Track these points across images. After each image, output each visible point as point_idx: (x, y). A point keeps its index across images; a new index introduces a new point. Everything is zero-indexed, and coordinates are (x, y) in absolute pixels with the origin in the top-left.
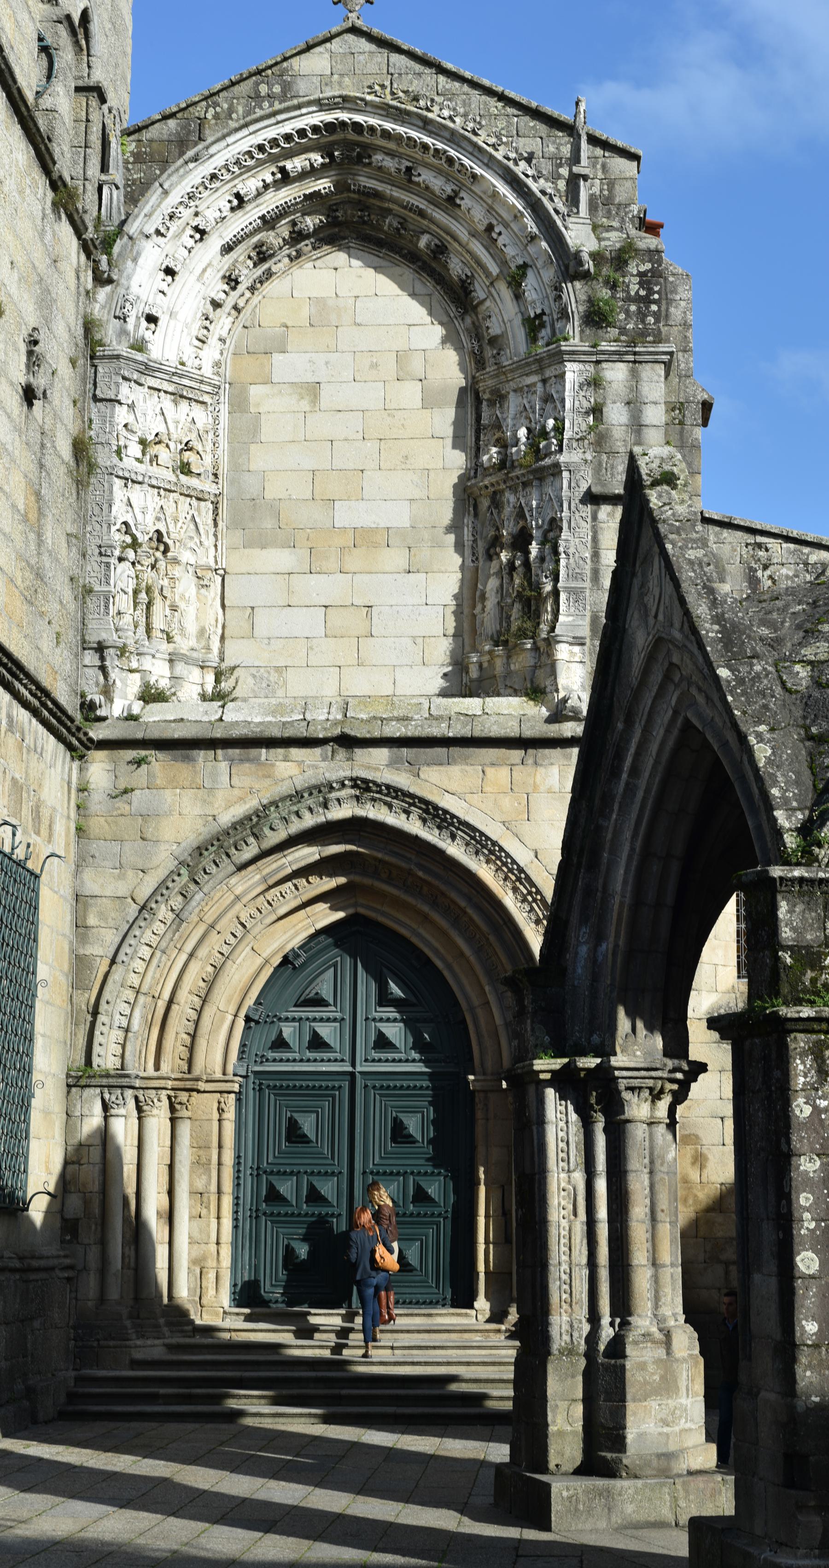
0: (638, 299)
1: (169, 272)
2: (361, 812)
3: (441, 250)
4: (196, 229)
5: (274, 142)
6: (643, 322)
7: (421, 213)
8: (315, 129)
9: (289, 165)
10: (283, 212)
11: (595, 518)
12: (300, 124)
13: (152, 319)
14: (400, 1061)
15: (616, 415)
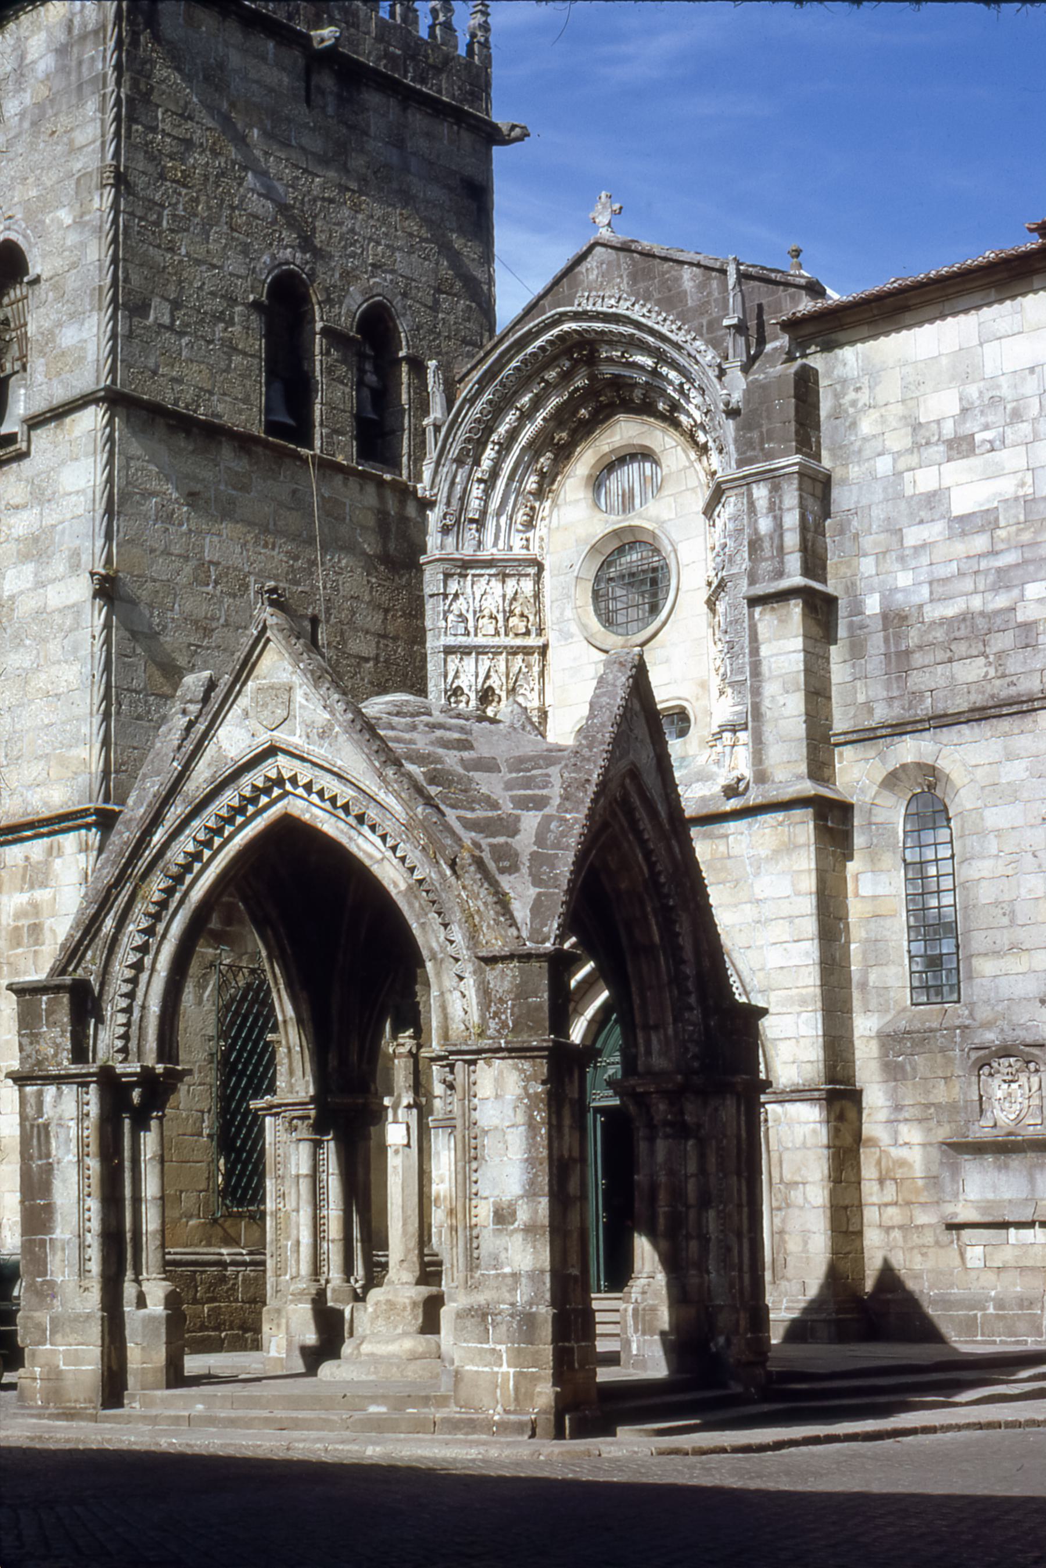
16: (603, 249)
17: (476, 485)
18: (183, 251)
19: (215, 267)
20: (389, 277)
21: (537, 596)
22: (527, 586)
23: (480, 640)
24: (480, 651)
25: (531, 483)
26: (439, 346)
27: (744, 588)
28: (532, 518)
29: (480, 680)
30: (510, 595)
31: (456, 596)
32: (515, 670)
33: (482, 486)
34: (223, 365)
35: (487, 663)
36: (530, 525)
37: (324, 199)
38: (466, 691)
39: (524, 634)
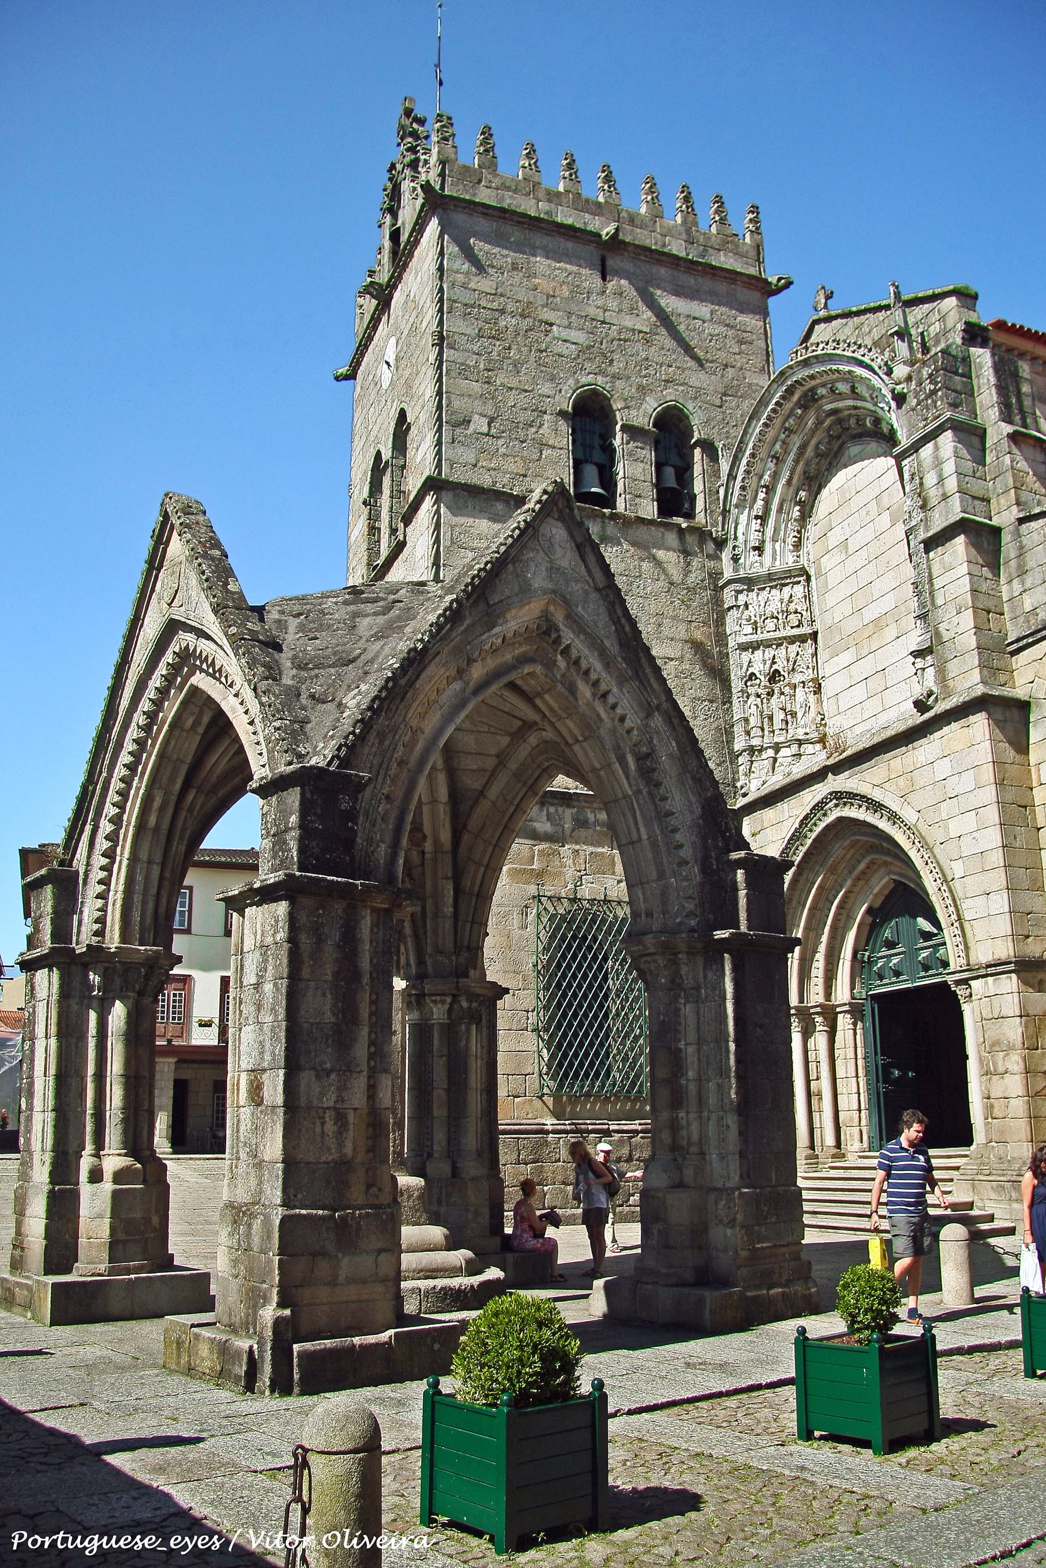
0: (933, 392)
1: (757, 517)
2: (839, 814)
3: (877, 421)
4: (763, 487)
5: (769, 418)
6: (935, 407)
7: (855, 408)
8: (783, 397)
9: (787, 425)
10: (803, 447)
11: (928, 558)
12: (774, 401)
13: (755, 548)
14: (934, 975)
15: (930, 479)
16: (823, 325)
17: (754, 521)
18: (498, 383)
19: (526, 391)
20: (681, 388)
21: (808, 597)
22: (799, 590)
23: (766, 636)
24: (767, 644)
25: (796, 512)
26: (728, 432)
27: (922, 535)
28: (800, 538)
29: (768, 666)
30: (786, 597)
31: (746, 606)
32: (792, 655)
33: (759, 521)
34: (536, 457)
35: (772, 652)
36: (798, 546)
37: (620, 340)
38: (758, 676)
39: (798, 626)
